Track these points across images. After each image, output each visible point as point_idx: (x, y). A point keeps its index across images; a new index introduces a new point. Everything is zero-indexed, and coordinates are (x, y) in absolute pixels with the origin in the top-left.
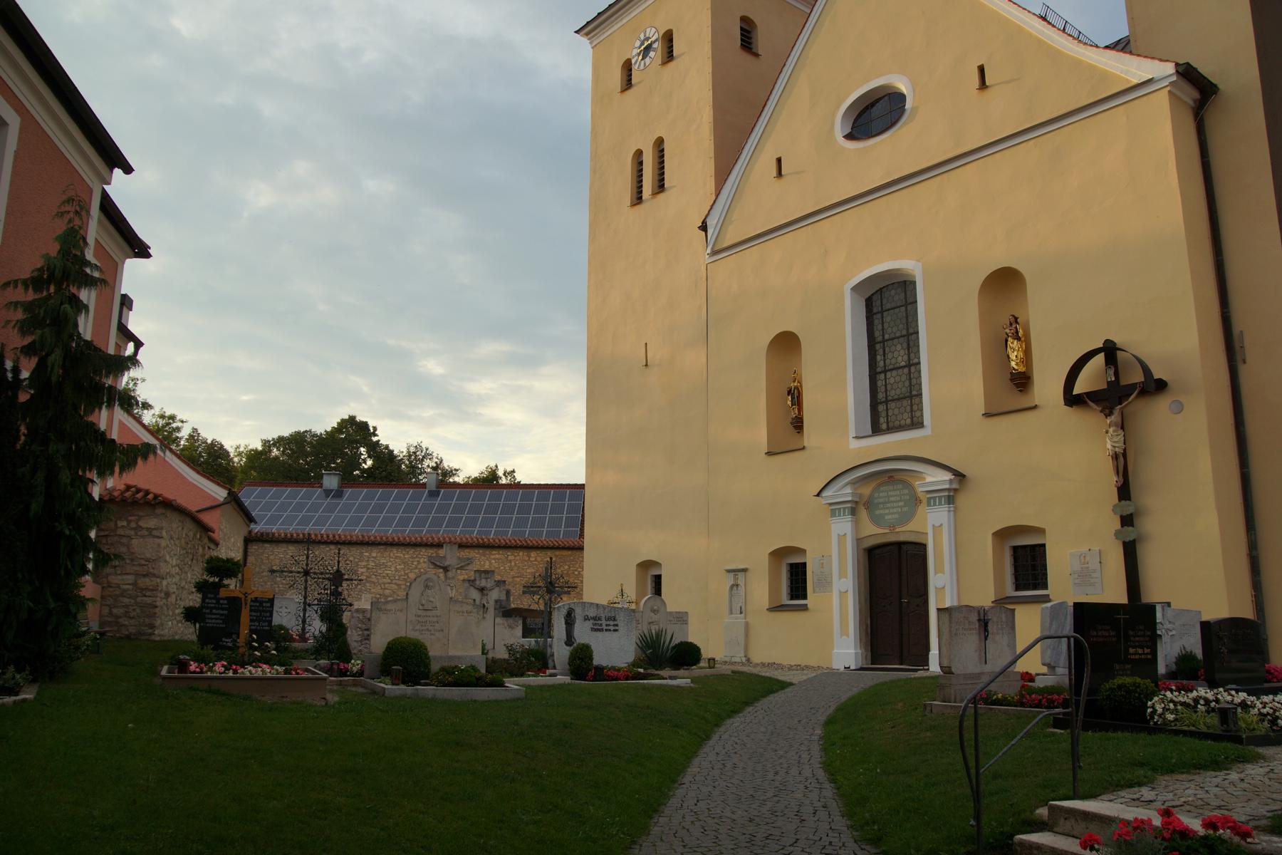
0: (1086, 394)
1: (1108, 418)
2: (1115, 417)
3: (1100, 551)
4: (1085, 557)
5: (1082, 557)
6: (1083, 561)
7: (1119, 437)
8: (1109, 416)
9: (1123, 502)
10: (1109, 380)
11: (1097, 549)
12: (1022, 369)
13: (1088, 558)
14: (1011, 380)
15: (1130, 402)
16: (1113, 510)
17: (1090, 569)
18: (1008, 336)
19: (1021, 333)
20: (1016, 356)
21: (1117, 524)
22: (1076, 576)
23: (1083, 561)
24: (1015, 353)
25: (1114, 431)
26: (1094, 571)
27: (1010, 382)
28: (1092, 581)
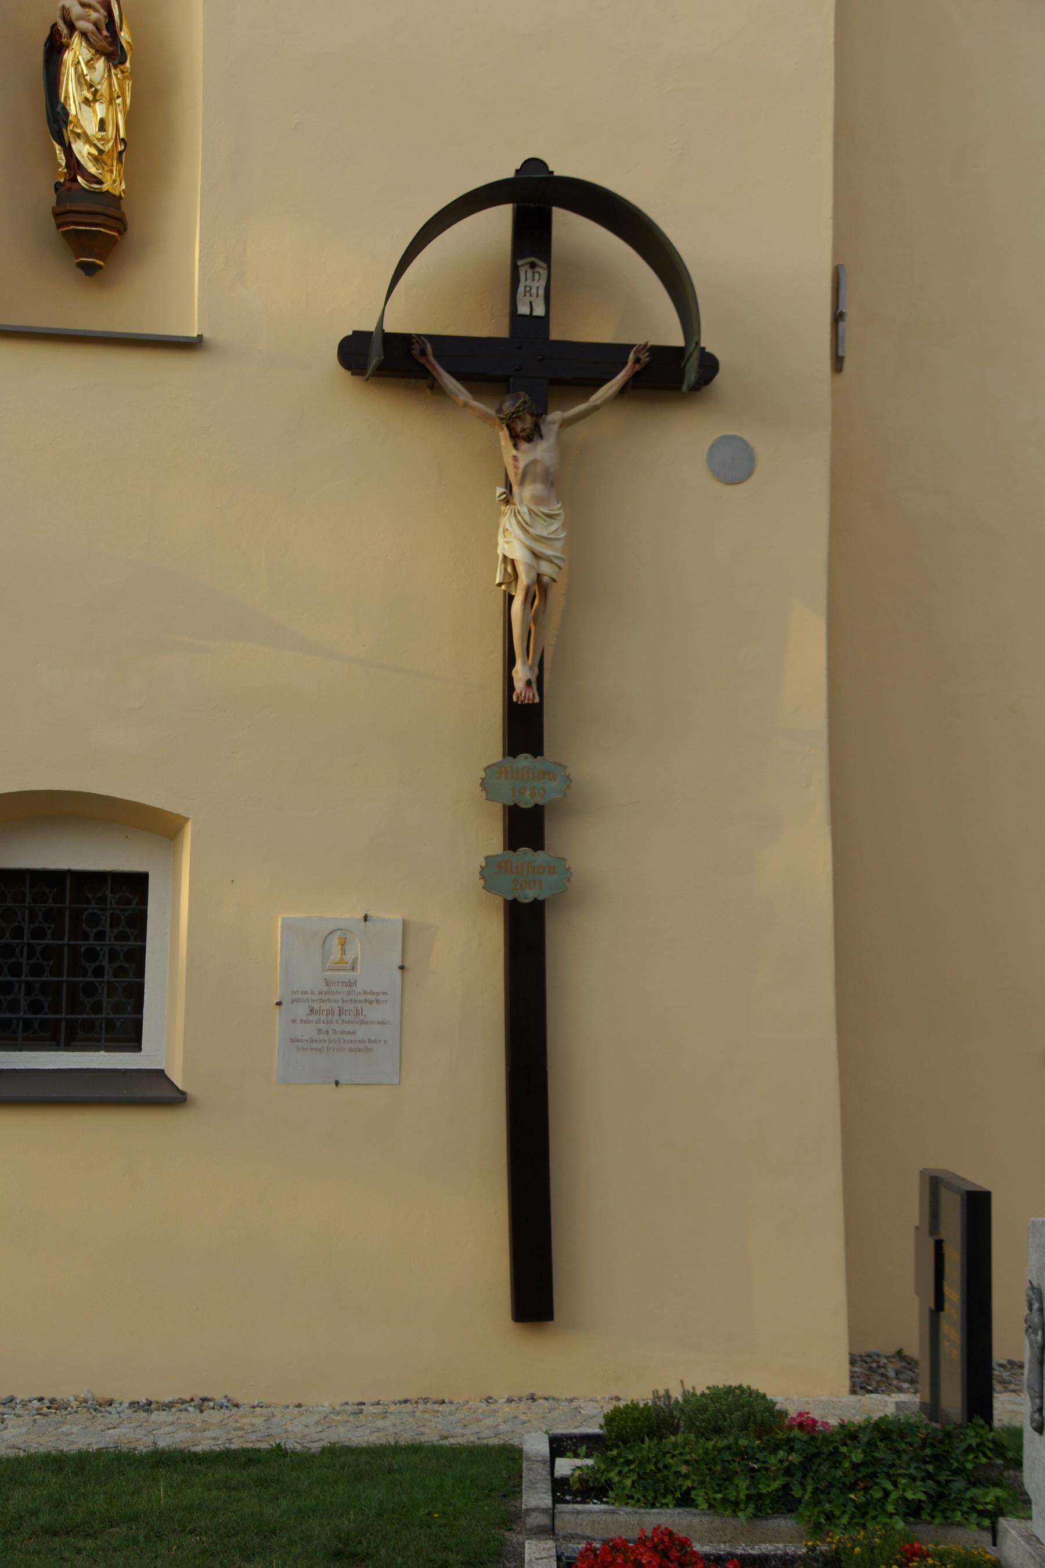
0: (435, 340)
1: (524, 446)
2: (541, 451)
3: (405, 925)
4: (343, 943)
5: (334, 942)
6: (336, 955)
7: (555, 525)
8: (529, 439)
9: (524, 761)
10: (523, 309)
11: (396, 916)
12: (113, 182)
13: (356, 949)
14: (56, 215)
15: (596, 408)
16: (483, 783)
17: (360, 988)
18: (72, 27)
19: (124, 36)
20: (102, 125)
21: (494, 841)
22: (302, 1011)
23: (336, 955)
24: (100, 109)
25: (538, 500)
26: (376, 998)
27: (52, 221)
28: (363, 1033)
